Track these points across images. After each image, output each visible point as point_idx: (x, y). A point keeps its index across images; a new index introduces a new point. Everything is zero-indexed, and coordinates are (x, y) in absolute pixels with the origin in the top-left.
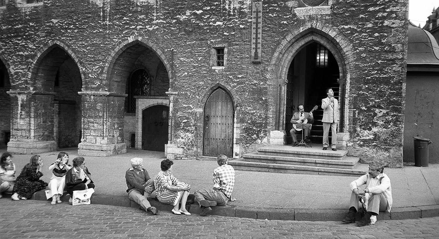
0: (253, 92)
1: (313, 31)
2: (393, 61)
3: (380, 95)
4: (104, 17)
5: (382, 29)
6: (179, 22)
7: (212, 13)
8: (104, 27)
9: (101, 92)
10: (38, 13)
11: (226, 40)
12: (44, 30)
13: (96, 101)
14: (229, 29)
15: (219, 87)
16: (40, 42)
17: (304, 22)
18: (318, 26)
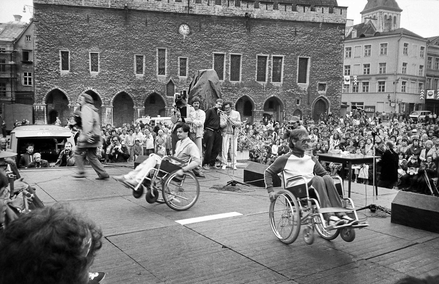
0: (307, 111)
1: (322, 97)
2: (339, 105)
3: (336, 112)
4: (263, 89)
5: (337, 98)
7: (297, 90)
8: (263, 91)
9: (261, 110)
10: (238, 85)
11: (301, 98)
12: (241, 90)
13: (259, 113)
14: (301, 95)
15: (298, 110)
16: (240, 94)
17: (319, 95)
18: (323, 96)
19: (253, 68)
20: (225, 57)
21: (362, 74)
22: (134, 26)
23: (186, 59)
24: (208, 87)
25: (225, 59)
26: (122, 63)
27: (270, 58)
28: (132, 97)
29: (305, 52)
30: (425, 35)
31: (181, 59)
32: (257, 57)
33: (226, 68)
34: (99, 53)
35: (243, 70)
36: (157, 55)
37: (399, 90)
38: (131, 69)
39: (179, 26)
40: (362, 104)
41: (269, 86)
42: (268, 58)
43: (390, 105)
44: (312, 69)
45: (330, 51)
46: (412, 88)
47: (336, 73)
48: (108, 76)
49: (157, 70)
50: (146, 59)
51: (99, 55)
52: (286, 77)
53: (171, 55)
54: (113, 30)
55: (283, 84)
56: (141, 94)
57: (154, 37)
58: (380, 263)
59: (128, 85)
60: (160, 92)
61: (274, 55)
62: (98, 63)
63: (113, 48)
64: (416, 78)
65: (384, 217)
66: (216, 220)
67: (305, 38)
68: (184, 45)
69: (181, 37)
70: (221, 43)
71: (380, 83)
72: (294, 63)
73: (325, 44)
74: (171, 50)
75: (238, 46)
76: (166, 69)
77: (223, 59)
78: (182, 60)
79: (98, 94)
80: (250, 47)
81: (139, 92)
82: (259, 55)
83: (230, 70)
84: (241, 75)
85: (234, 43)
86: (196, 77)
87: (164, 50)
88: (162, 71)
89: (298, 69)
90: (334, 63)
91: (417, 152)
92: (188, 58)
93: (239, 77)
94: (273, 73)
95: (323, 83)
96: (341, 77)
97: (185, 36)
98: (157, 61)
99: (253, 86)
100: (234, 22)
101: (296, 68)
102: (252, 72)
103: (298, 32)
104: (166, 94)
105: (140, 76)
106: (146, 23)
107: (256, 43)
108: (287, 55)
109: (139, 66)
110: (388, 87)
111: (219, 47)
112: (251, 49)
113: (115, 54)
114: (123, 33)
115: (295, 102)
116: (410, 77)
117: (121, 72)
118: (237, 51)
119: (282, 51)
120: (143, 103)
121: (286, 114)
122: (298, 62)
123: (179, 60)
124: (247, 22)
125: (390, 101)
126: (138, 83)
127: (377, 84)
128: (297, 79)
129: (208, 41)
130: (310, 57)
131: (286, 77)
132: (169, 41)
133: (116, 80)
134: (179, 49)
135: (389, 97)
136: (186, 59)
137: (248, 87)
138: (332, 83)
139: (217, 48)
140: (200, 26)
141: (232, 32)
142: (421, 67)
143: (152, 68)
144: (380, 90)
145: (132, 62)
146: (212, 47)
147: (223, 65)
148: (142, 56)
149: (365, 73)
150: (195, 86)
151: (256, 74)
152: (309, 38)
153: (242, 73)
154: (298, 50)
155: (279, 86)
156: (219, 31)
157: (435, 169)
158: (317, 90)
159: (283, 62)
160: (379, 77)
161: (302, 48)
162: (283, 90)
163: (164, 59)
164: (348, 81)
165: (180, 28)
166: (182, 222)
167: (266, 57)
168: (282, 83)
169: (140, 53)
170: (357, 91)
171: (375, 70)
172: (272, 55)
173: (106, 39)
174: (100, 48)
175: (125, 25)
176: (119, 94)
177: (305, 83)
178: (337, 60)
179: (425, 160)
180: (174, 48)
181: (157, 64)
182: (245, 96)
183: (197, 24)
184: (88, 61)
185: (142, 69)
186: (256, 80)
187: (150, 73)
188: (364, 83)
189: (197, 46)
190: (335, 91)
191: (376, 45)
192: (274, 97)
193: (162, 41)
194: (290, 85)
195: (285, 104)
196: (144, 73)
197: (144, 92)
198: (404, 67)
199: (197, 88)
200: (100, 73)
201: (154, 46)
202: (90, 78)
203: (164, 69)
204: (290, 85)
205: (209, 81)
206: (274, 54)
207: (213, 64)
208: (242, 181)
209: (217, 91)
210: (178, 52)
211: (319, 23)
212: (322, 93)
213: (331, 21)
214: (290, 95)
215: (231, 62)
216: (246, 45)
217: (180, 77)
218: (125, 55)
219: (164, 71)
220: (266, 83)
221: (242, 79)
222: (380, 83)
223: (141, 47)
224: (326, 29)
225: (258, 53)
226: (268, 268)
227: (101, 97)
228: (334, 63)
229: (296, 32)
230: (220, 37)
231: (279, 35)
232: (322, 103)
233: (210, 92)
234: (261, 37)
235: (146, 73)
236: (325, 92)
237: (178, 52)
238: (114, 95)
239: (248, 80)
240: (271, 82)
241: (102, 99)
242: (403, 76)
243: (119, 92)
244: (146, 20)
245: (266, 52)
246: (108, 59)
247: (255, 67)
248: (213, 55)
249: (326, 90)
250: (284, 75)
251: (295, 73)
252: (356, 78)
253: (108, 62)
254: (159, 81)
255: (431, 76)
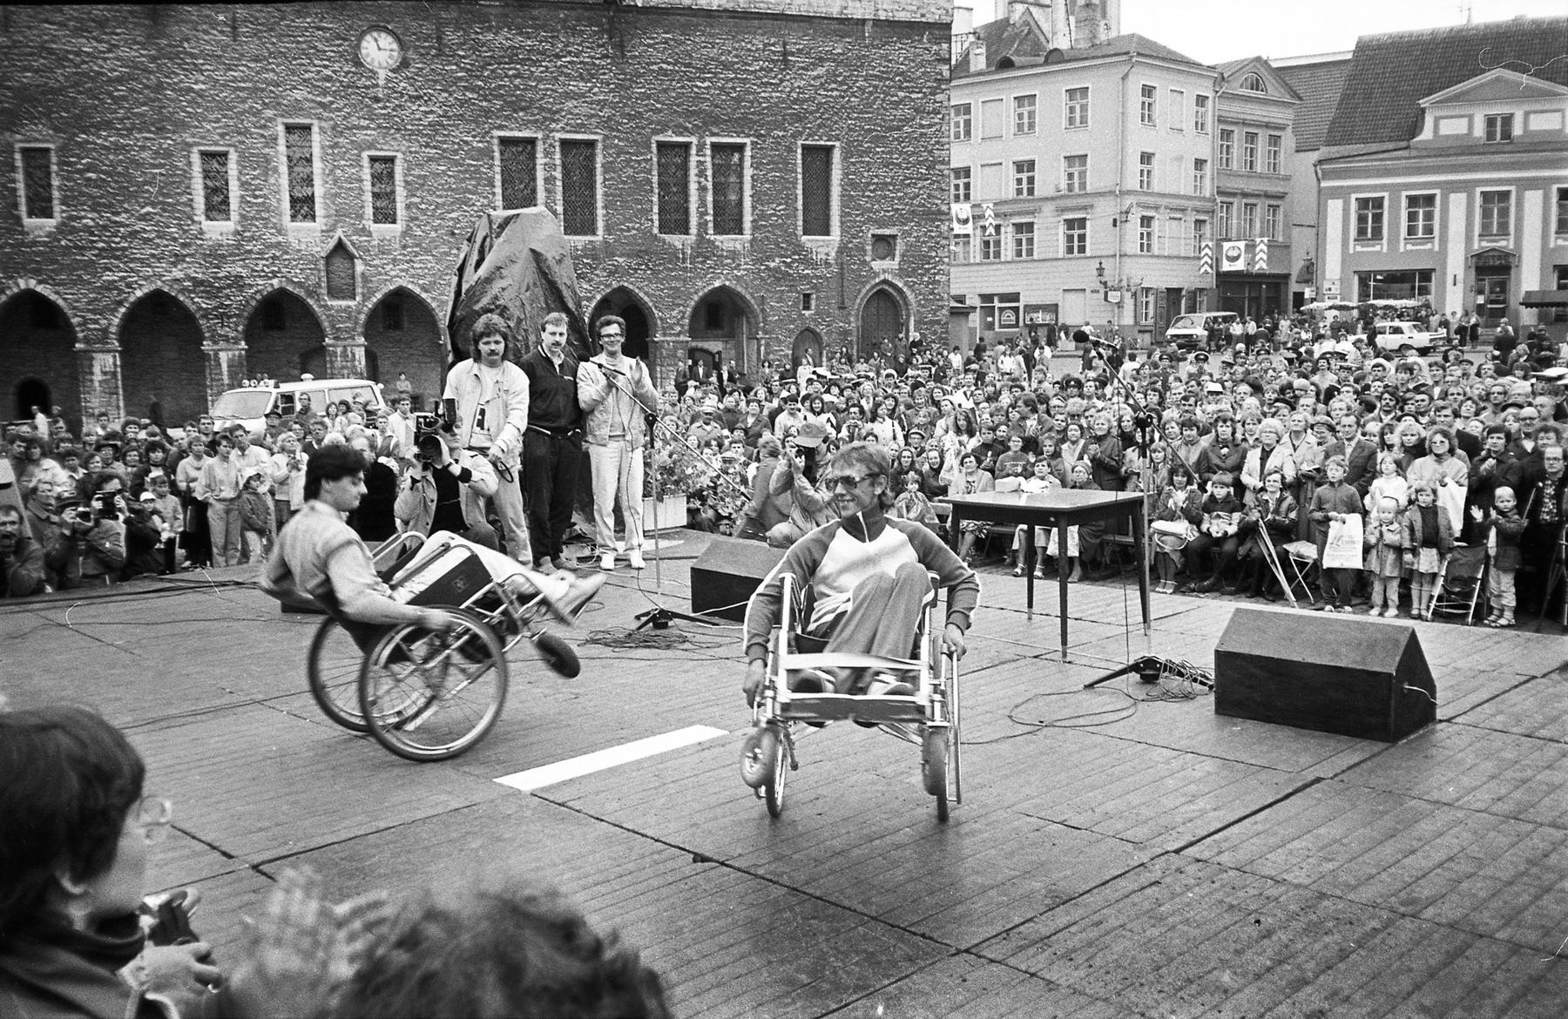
1: (885, 282)
3: (935, 333)
4: (684, 260)
5: (934, 282)
6: (768, 268)
9: (682, 338)
10: (594, 249)
11: (815, 287)
12: (604, 269)
13: (676, 349)
15: (807, 329)
17: (877, 274)
19: (642, 186)
20: (540, 147)
21: (1012, 194)
22: (188, 40)
23: (391, 160)
24: (531, 276)
25: (539, 155)
26: (146, 183)
27: (701, 148)
28: (193, 308)
29: (820, 126)
30: (1207, 56)
31: (373, 159)
32: (654, 146)
33: (547, 190)
34: (52, 146)
35: (606, 194)
36: (282, 148)
37: (1132, 246)
38: (185, 204)
39: (360, 38)
40: (1015, 297)
41: (704, 250)
42: (693, 151)
43: (1106, 299)
44: (849, 184)
45: (907, 121)
46: (1172, 235)
47: (930, 196)
48: (92, 234)
49: (286, 204)
50: (238, 163)
51: (53, 154)
52: (762, 216)
53: (336, 145)
54: (105, 59)
55: (753, 242)
56: (228, 297)
57: (265, 81)
58: (1225, 858)
59: (174, 264)
60: (300, 284)
61: (715, 139)
62: (50, 185)
63: (108, 125)
64: (1186, 203)
65: (1187, 697)
66: (639, 762)
67: (818, 77)
68: (385, 108)
69: (368, 78)
70: (520, 98)
71: (1070, 224)
72: (785, 165)
73: (887, 94)
74: (333, 128)
75: (585, 110)
76: (318, 200)
77: (533, 157)
78: (377, 165)
79: (60, 302)
80: (627, 110)
81: (220, 289)
82: (661, 138)
83: (559, 196)
84: (600, 212)
85: (568, 96)
86: (479, 240)
87: (307, 128)
88: (303, 206)
89: (800, 187)
90: (920, 163)
91: (1230, 462)
92: (400, 155)
93: (593, 221)
94: (714, 201)
95: (887, 232)
96: (944, 208)
97: (382, 74)
98: (284, 169)
99: (646, 252)
100: (565, 21)
101: (795, 183)
102: (639, 202)
103: (793, 54)
104: (324, 291)
105: (218, 231)
106: (234, 28)
107: (649, 97)
108: (759, 136)
109: (215, 191)
110: (1098, 234)
111: (515, 111)
112: (631, 117)
113: (118, 148)
114: (145, 70)
115: (796, 304)
116: (1164, 202)
117: (143, 218)
118: (583, 125)
119: (741, 125)
120: (240, 328)
121: (767, 345)
122: (799, 161)
123: (366, 162)
124: (611, 21)
125: (1105, 284)
126: (216, 255)
127: (1062, 228)
128: (800, 223)
129: (472, 90)
130: (837, 144)
131: (762, 216)
132: (325, 93)
133: (124, 249)
134: (364, 123)
135: (1101, 271)
136: (391, 160)
137: (629, 256)
138: (917, 231)
139: (507, 118)
140: (439, 39)
141: (558, 57)
142: (1200, 163)
143: (265, 196)
144: (1070, 250)
145: (186, 175)
146: (487, 113)
147: (534, 180)
148: (225, 155)
149: (1019, 192)
150: (482, 271)
151: (656, 209)
152: (832, 76)
153: (606, 207)
154: (799, 118)
155: (739, 247)
156: (512, 56)
157: (1293, 515)
158: (868, 259)
159: (748, 162)
160: (1062, 203)
161: (811, 113)
162: (755, 262)
163: (309, 160)
164: (966, 221)
165: (364, 44)
166: (526, 781)
167: (687, 146)
168: (747, 236)
169: (216, 144)
170: (997, 255)
171: (1050, 178)
172: (709, 140)
173: (80, 93)
174: (57, 130)
175: (149, 37)
176: (141, 302)
177: (828, 234)
178: (930, 152)
179: (1261, 485)
180: (345, 118)
181: (284, 181)
182: (622, 289)
183: (428, 28)
184: (14, 181)
185: (226, 202)
186: (656, 231)
187: (257, 213)
188: (1019, 227)
189: (432, 112)
190: (927, 259)
191: (1051, 93)
192: (723, 288)
193: (298, 95)
194: (777, 245)
195: (763, 310)
196: (234, 216)
197: (241, 288)
198: (1146, 167)
199: (488, 280)
200: (63, 224)
201: (269, 113)
202: (23, 244)
203: (310, 200)
204: (777, 245)
205: (533, 251)
206: (713, 134)
207: (498, 177)
208: (686, 608)
209: (563, 288)
210: (361, 136)
211: (864, 21)
212: (885, 268)
213: (902, 16)
214: (778, 279)
215: (564, 165)
216: (613, 106)
217: (374, 227)
218: (156, 153)
219: (312, 209)
220: (691, 238)
221: (608, 229)
222: (1070, 224)
223: (218, 121)
224: (887, 43)
225: (655, 132)
226: (873, 918)
227: (70, 313)
228: (920, 163)
229: (785, 54)
230: (516, 76)
231: (727, 66)
232: (886, 300)
233: (539, 291)
234: (665, 73)
235: (243, 217)
236: (893, 264)
237: (361, 136)
238: (120, 303)
239: (629, 230)
240: (711, 235)
241: (75, 321)
242: (1143, 199)
243: (139, 293)
244: (234, 20)
245: (686, 129)
246: (89, 168)
247: (650, 182)
248: (496, 141)
249: (897, 259)
250: (754, 208)
251: (790, 201)
252: (989, 213)
253: (89, 179)
254: (295, 245)
255: (1234, 195)
